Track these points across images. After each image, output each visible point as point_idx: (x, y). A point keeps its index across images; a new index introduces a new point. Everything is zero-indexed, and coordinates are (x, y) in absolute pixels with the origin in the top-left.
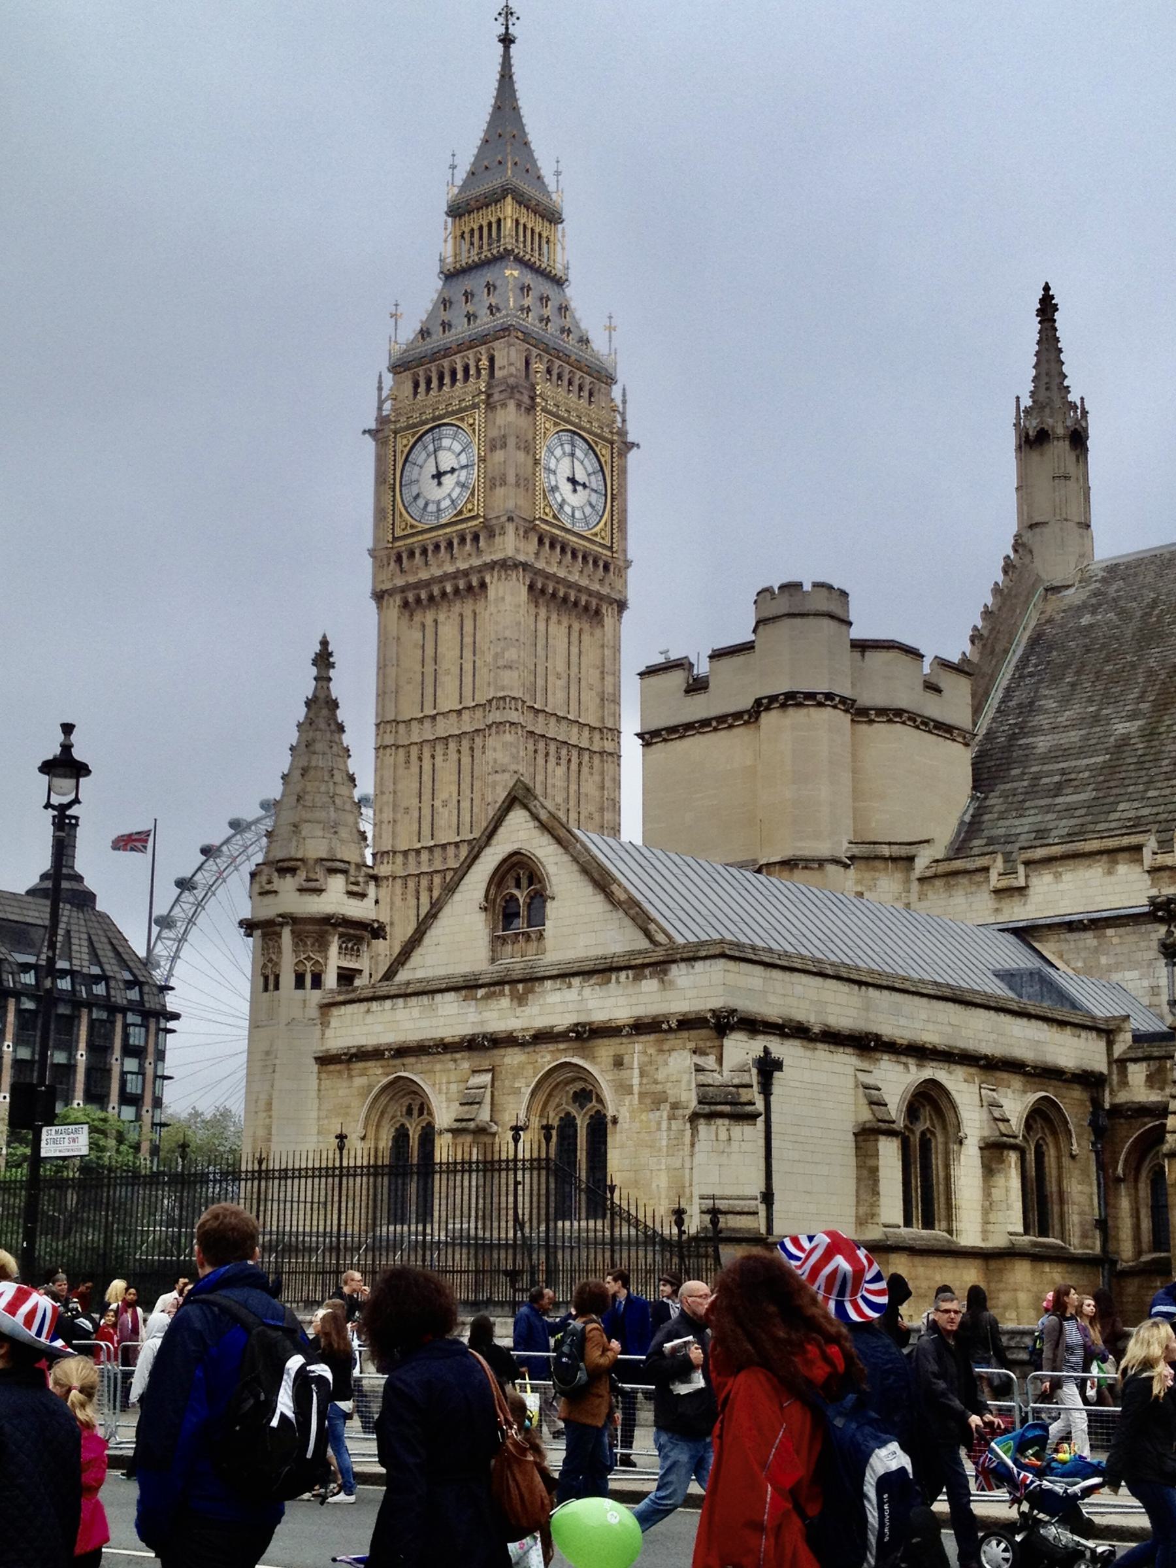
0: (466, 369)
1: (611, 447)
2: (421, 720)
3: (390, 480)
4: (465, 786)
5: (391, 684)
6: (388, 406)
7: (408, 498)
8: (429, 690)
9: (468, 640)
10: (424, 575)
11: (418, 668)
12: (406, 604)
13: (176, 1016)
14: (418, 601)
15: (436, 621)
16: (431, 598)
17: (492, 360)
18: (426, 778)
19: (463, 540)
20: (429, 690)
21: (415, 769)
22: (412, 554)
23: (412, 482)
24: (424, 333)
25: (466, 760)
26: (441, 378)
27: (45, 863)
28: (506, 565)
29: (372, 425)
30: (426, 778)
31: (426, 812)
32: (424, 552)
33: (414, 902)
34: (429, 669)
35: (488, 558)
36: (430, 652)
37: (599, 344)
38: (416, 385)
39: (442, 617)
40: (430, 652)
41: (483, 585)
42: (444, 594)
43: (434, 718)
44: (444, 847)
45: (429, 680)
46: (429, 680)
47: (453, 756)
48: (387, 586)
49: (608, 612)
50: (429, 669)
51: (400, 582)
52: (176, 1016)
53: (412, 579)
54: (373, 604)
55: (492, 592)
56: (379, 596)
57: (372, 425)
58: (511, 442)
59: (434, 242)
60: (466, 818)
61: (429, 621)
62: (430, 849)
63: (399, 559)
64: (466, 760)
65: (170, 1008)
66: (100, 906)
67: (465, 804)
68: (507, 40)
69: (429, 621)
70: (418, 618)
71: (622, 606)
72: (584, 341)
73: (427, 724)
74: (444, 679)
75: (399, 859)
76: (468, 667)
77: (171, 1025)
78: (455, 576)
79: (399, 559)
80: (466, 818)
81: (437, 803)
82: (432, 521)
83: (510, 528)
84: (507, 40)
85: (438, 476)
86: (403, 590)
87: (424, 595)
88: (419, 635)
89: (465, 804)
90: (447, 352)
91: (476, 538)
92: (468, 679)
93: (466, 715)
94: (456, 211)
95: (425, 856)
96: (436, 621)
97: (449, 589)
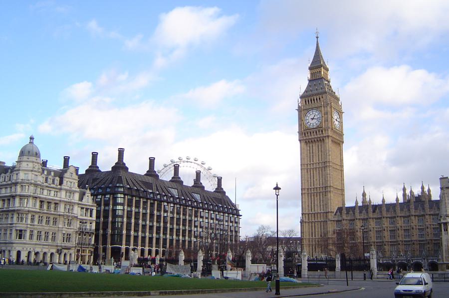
0: (317, 99)
1: (340, 113)
2: (310, 164)
3: (301, 119)
4: (321, 177)
5: (303, 157)
6: (300, 105)
7: (306, 123)
9: (320, 150)
10: (310, 137)
11: (309, 154)
12: (306, 142)
13: (241, 216)
14: (309, 141)
15: (312, 146)
18: (312, 175)
19: (319, 131)
21: (309, 173)
22: (308, 133)
23: (307, 120)
24: (306, 91)
25: (321, 172)
26: (311, 101)
27: (216, 186)
28: (328, 136)
29: (297, 108)
30: (312, 175)
31: (312, 181)
32: (311, 133)
33: (310, 198)
34: (311, 154)
35: (325, 135)
37: (336, 94)
38: (306, 102)
39: (314, 145)
41: (323, 139)
42: (314, 141)
43: (313, 164)
44: (317, 188)
45: (311, 157)
46: (311, 157)
47: (318, 171)
48: (302, 139)
49: (341, 143)
50: (311, 154)
51: (305, 138)
52: (241, 216)
53: (307, 138)
54: (299, 142)
55: (325, 141)
56: (300, 141)
57: (297, 108)
58: (329, 114)
59: (307, 75)
60: (321, 183)
61: (311, 145)
62: (314, 188)
63: (305, 134)
64: (321, 172)
65: (240, 214)
66: (226, 195)
67: (321, 180)
68: (317, 38)
70: (308, 145)
71: (343, 142)
72: (334, 93)
73: (311, 165)
74: (314, 156)
75: (306, 190)
76: (320, 155)
77: (240, 217)
78: (318, 137)
79: (305, 134)
80: (321, 183)
81: (315, 180)
82: (311, 127)
83: (329, 129)
84: (317, 38)
85: (313, 119)
86: (306, 139)
87: (310, 141)
88: (308, 148)
89: (321, 180)
90: (313, 95)
91: (322, 131)
92: (320, 157)
93: (320, 164)
94: (310, 69)
95: (312, 189)
96: (312, 146)
97: (316, 140)
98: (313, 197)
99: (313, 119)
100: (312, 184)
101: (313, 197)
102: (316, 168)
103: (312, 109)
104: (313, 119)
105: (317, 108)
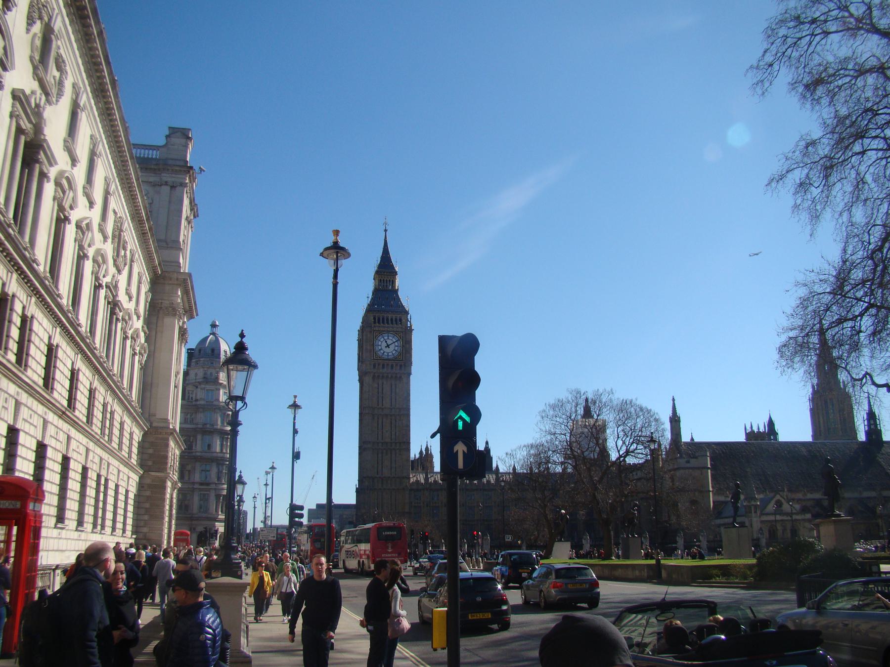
8: (380, 401)
12: (374, 377)
16: (383, 377)
17: (400, 320)
20: (380, 401)
25: (393, 422)
36: (380, 390)
40: (380, 390)
41: (400, 377)
42: (387, 377)
60: (393, 437)
61: (380, 382)
68: (386, 231)
69: (380, 382)
80: (393, 437)
84: (386, 231)
85: (388, 346)
91: (401, 366)
92: (393, 400)
98: (380, 455)
99: (387, 346)
100: (380, 438)
101: (380, 455)
102: (387, 415)
103: (388, 332)
104: (388, 346)
105: (396, 333)
